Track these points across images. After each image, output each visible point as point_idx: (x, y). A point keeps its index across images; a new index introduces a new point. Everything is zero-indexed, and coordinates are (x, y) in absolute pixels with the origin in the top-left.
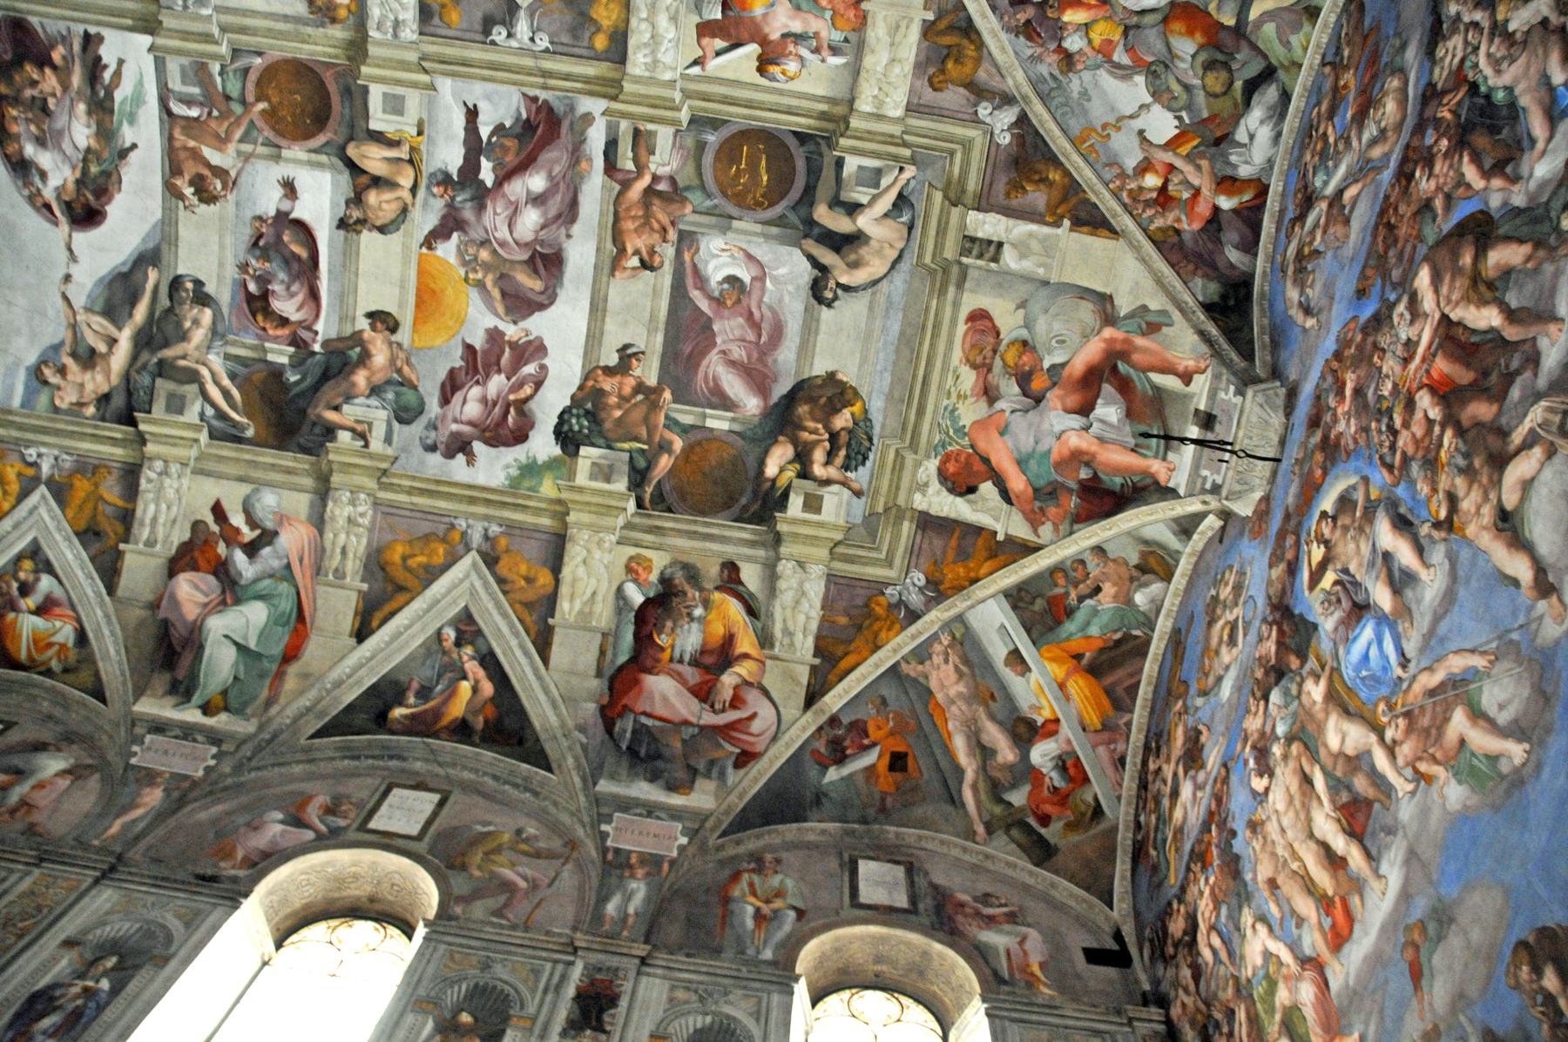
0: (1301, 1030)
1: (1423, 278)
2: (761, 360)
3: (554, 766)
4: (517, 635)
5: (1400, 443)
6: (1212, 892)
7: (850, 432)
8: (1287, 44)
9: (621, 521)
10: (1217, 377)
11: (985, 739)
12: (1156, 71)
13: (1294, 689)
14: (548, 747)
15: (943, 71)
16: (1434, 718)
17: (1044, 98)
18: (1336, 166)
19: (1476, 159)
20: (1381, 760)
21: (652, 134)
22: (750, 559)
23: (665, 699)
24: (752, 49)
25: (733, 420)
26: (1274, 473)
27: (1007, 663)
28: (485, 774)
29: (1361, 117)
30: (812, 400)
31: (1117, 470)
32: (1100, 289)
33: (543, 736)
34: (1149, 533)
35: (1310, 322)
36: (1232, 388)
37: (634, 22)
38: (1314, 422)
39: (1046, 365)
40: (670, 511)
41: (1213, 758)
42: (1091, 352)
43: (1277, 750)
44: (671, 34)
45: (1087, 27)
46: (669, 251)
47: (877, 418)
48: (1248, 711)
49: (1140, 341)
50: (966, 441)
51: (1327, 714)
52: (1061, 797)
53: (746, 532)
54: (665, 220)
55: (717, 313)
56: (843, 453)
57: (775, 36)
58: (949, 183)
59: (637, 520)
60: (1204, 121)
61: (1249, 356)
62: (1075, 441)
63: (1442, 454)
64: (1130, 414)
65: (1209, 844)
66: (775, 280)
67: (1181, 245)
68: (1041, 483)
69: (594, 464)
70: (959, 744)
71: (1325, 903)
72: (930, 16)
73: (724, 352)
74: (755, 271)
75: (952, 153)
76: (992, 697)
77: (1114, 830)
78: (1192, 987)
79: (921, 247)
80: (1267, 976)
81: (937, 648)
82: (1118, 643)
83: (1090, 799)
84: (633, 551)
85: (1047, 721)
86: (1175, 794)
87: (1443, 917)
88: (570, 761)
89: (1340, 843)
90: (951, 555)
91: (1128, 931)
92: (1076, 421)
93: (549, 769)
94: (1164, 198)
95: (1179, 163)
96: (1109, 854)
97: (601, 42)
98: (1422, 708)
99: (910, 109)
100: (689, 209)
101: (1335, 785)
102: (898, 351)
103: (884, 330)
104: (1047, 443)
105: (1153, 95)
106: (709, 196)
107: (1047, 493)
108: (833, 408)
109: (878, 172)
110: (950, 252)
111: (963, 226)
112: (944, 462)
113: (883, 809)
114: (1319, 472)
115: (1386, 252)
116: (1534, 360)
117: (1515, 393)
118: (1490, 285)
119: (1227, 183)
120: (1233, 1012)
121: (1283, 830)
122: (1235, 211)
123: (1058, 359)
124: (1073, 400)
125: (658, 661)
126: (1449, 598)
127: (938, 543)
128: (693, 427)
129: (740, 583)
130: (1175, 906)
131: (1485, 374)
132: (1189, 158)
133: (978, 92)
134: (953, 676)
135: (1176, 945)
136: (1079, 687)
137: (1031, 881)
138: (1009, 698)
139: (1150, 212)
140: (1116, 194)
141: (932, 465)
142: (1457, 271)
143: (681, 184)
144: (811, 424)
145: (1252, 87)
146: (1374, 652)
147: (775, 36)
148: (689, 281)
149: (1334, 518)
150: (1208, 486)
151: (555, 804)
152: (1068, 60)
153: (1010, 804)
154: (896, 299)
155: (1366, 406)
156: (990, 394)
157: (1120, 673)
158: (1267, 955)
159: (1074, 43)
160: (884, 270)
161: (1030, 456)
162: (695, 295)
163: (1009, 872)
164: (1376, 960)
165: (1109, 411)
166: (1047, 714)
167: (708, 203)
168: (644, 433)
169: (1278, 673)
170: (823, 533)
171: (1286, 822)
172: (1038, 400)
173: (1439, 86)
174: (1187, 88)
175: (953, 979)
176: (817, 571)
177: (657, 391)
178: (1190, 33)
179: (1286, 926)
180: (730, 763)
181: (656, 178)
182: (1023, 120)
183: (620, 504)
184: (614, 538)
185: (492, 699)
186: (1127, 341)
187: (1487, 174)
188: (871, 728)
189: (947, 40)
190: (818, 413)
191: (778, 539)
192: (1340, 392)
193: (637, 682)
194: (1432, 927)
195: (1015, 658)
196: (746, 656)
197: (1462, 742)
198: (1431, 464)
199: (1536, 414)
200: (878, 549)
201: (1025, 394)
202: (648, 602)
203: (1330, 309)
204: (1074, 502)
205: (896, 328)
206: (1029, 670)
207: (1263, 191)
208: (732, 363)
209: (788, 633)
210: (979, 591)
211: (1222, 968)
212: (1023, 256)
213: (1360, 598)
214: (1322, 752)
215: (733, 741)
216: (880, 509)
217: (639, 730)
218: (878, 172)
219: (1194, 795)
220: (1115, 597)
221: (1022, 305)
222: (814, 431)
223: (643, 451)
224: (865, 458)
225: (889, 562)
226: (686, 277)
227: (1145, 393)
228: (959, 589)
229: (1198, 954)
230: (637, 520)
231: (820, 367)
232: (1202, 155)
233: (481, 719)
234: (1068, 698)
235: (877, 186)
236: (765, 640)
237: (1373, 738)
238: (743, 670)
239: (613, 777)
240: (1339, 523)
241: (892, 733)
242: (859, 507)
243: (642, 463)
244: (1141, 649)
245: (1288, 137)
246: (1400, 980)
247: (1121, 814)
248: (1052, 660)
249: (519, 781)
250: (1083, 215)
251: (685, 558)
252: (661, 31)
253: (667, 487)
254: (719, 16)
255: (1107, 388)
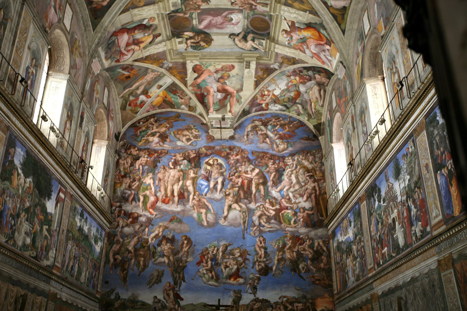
0: (147, 200)
1: (257, 171)
2: (213, 26)
3: (95, 31)
4: (123, 4)
5: (234, 177)
6: (147, 161)
7: (200, 46)
8: (293, 111)
9: (163, 12)
10: (232, 119)
11: (140, 87)
12: (288, 90)
13: (189, 167)
14: (99, 26)
15: (285, 59)
16: (202, 206)
17: (281, 72)
18: (272, 132)
19: (275, 176)
20: (191, 197)
21: (267, 7)
22: (163, 37)
23: (123, 40)
24: (289, 30)
25: (196, 24)
26: (219, 139)
27: (158, 85)
28: (82, 14)
29: (281, 138)
30: (206, 37)
31: (208, 101)
32: (244, 88)
33: (101, 23)
34: (198, 108)
35: (245, 137)
36: (231, 123)
37: (295, 10)
38: (231, 149)
39: (226, 81)
40: (169, 19)
41: (167, 146)
42: (230, 89)
43: (178, 168)
44: (292, 16)
45: (296, 80)
46: (237, 7)
47: (205, 50)
48: (180, 154)
49: (235, 99)
50: (205, 69)
51: (190, 179)
52: (136, 105)
53: (169, 33)
54: (245, 7)
55: (223, 17)
56: (195, 45)
57: (292, 34)
58: (261, 57)
59: (164, 15)
60: (278, 99)
61: (237, 122)
62: (212, 90)
63: (234, 189)
64: (220, 100)
65: (153, 155)
66: (233, 27)
67: (254, 101)
68: (201, 85)
69: (176, 2)
70: (137, 84)
71: (166, 196)
72: (297, 59)
73: (213, 19)
74: (235, 23)
75: (268, 58)
76: (150, 85)
77: (135, 117)
78: (129, 165)
79: (246, 53)
80: (147, 187)
81: (156, 73)
82: (172, 104)
83: (138, 110)
84: (156, 17)
85: (149, 96)
86: (153, 135)
87: (180, 222)
88: (99, 35)
89: (176, 194)
90: (178, 70)
91: (121, 134)
92: (216, 90)
93: (94, 31)
94: (263, 96)
95: (270, 97)
96: (131, 119)
97: (290, 2)
98: (202, 202)
99: (277, 54)
100: (249, 12)
101: (182, 188)
102: (221, 52)
103: (226, 49)
104: (210, 85)
105: (283, 90)
106: (252, 15)
107: (199, 86)
108: (204, 41)
109: (262, 45)
110: (246, 59)
111: (252, 61)
112: (199, 65)
113: (116, 80)
114: (223, 155)
115: (260, 157)
116: (250, 203)
117: (246, 201)
118: (258, 188)
119: (267, 105)
120: (135, 181)
121: (169, 177)
122: (262, 107)
123: (227, 83)
124: (220, 88)
125: (131, 33)
126: (217, 200)
127: (180, 67)
128: (192, 18)
129: (157, 38)
130: (136, 149)
131: (247, 193)
132: (271, 98)
133: (281, 65)
134: (151, 77)
135: (131, 154)
136: (159, 99)
137: (117, 110)
138: (151, 87)
139: (260, 94)
140: (263, 87)
141: (197, 63)
142: (259, 179)
143: (255, 10)
144: (200, 38)
145: (285, 106)
146: (204, 187)
147: (292, 34)
148: (230, 11)
149: (218, 164)
150: (212, 123)
151: (87, 37)
152: (289, 76)
153: (129, 97)
154: (234, 50)
155: (236, 164)
156: (217, 72)
157: (166, 105)
158: (150, 184)
159: (292, 77)
160: (240, 46)
161: (206, 82)
162: (227, 13)
163: (116, 105)
164: (167, 212)
165: (220, 96)
166: (151, 95)
167: (250, 15)
168: (188, 9)
169: (190, 161)
170: (174, 46)
171: (170, 177)
172: (218, 81)
173: (285, 160)
174: (285, 95)
175: (102, 128)
176: (165, 48)
177: (199, 9)
178: (295, 95)
179: (158, 188)
180: (116, 60)
181: (256, 6)
182: (276, 70)
183: (167, 10)
184: (158, 12)
185: (103, 6)
186: (234, 96)
187: (273, 181)
188: (133, 71)
189: (292, 60)
190: (202, 39)
191: (169, 39)
192: (237, 155)
193: (124, 33)
194: (178, 220)
195: (160, 87)
196: (140, 46)
197: (201, 213)
198: (233, 187)
199: (244, 206)
200: (174, 56)
201: (219, 79)
202: (145, 25)
203: (249, 144)
204: (199, 92)
205: (227, 51)
206: (159, 89)
207: (266, 110)
208: (210, 21)
209: (148, 50)
210: (173, 77)
211: (138, 173)
212: (248, 73)
213: (210, 179)
214: (185, 181)
215: (120, 56)
216: (184, 54)
217: (114, 42)
218: (262, 45)
219: (157, 143)
220: (181, 102)
221: (237, 74)
222: (198, 39)
223: (183, 10)
224: (195, 50)
225: (172, 59)
226: (232, 11)
227: (225, 103)
228: (171, 73)
229: (135, 163)
230: (164, 15)
231: (214, 37)
232: (272, 100)
233: (96, 6)
234: (156, 98)
235: (259, 45)
236: (145, 48)
237: (193, 193)
238: (136, 48)
239: (102, 48)
240: (218, 166)
241: (134, 74)
242: (183, 50)
243: (179, 11)
244: (172, 108)
245: (276, 112)
246: (169, 218)
247: (139, 117)
248: (163, 93)
249: (86, 24)
250: (258, 82)
251: (158, 26)
252: (293, 14)
253: (175, 17)
254: (296, 25)
255: (224, 94)
